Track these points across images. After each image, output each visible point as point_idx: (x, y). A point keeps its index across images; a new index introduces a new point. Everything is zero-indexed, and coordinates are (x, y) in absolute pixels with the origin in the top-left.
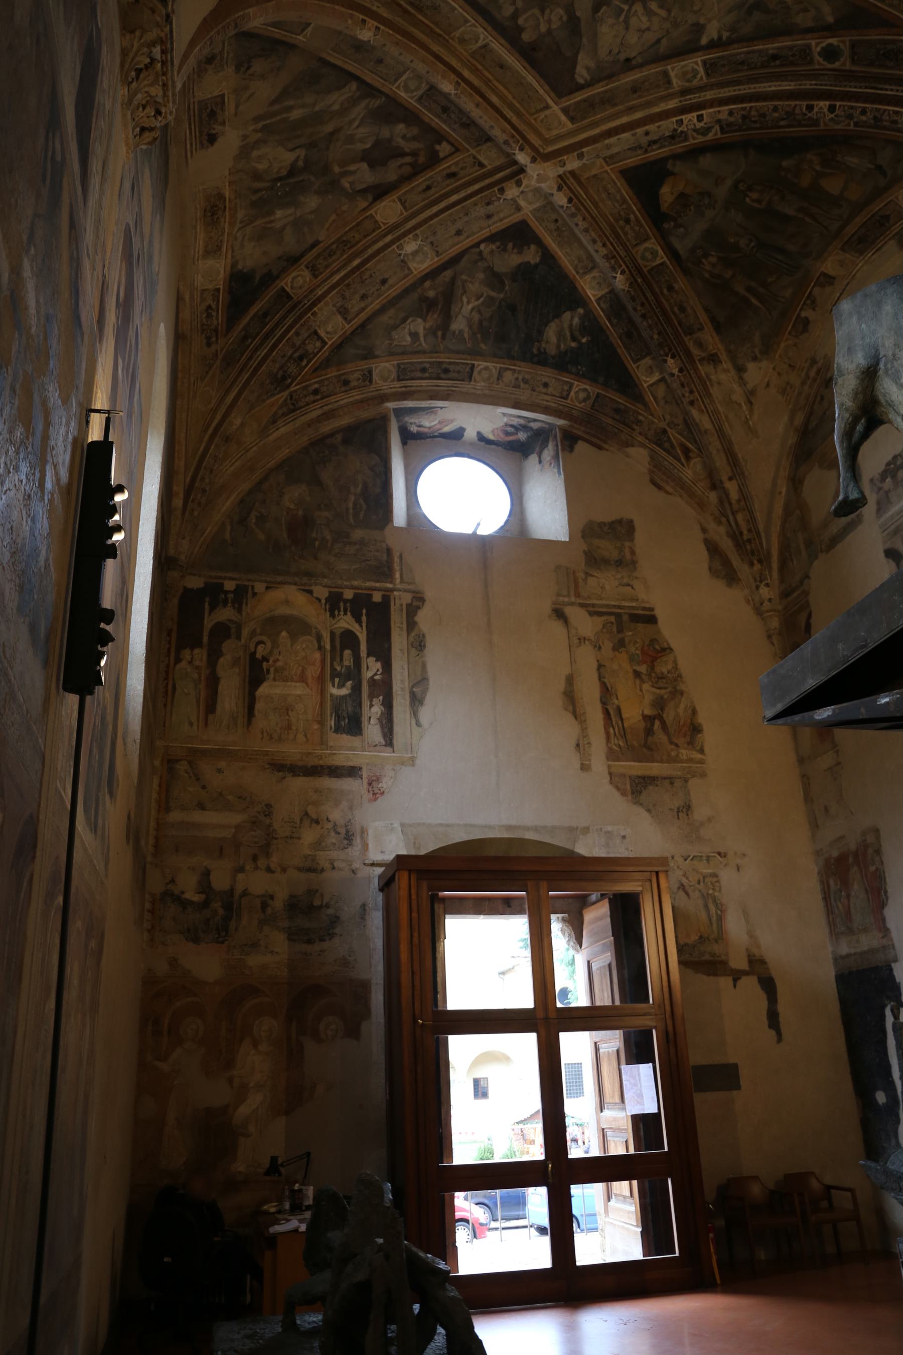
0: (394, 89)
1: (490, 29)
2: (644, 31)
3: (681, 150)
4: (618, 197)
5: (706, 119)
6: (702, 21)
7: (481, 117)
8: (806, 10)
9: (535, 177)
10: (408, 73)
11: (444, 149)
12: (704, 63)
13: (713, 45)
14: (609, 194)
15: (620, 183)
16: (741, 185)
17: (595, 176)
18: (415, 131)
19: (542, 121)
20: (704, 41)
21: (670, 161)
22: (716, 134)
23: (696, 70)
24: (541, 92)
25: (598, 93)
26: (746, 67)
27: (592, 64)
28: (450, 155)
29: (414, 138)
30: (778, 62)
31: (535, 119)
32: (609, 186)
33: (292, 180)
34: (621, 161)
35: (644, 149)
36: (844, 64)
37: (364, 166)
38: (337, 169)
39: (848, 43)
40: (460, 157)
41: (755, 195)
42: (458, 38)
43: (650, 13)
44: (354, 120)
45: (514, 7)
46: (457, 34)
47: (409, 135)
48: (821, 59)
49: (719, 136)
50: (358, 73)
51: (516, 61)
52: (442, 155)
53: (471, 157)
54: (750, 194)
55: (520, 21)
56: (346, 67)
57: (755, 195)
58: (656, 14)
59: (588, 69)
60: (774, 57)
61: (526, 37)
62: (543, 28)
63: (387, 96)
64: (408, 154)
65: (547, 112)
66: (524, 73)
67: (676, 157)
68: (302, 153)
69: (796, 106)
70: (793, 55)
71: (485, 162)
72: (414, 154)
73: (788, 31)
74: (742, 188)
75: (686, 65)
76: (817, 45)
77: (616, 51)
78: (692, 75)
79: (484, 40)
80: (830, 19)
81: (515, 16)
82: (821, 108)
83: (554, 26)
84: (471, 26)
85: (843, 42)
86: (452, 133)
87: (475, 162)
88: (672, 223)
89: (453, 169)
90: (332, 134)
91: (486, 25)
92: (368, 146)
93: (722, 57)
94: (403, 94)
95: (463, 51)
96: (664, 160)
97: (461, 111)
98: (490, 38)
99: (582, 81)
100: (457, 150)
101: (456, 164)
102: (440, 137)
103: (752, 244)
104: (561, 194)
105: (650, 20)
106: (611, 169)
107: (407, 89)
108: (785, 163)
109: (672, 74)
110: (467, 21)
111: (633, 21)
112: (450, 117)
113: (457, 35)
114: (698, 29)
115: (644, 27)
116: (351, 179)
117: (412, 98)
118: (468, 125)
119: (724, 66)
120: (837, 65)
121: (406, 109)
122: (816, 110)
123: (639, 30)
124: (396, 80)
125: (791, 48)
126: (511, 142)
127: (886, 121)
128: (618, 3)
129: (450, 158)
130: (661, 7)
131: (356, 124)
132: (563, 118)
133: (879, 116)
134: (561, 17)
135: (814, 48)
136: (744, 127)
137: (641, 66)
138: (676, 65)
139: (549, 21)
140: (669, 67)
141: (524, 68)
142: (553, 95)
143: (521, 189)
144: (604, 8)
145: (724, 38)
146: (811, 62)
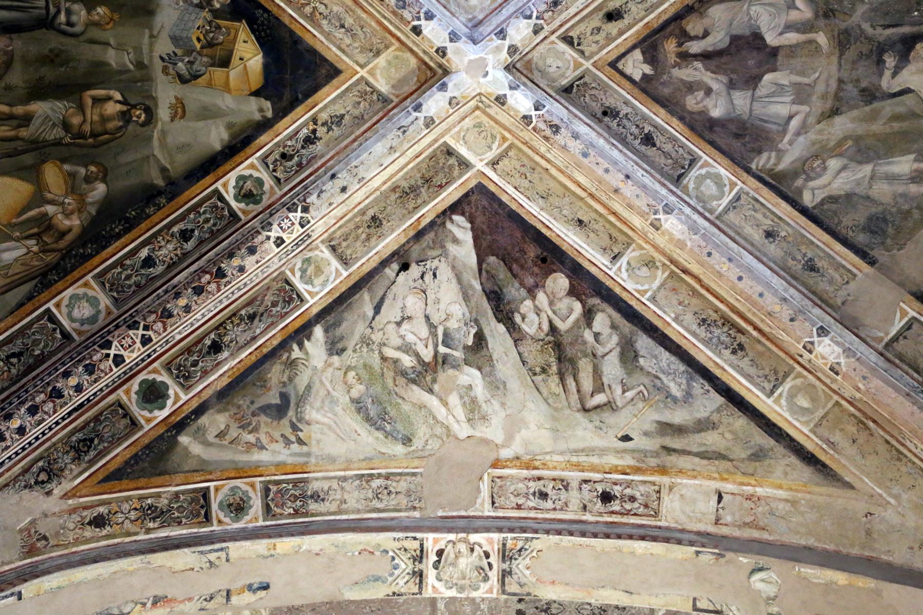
0: (739, 182)
1: (617, 290)
2: (403, 319)
3: (263, 139)
4: (324, 22)
5: (271, 244)
6: (336, 358)
7: (607, 171)
8: (221, 435)
9: (489, 69)
10: (721, 208)
11: (636, 66)
12: (302, 300)
13: (302, 333)
14: (342, 26)
15: (331, 52)
16: (143, 117)
17: (378, 53)
18: (692, 102)
19: (493, 137)
20: (318, 331)
21: (269, 114)
22: (225, 185)
23: (306, 283)
24: (510, 190)
25: (425, 203)
26: (243, 312)
27: (452, 248)
28: (624, 55)
29: (691, 87)
30: (208, 342)
31: (504, 139)
32: (348, 41)
33: (906, 30)
34: (347, 89)
35: (319, 123)
36: (127, 392)
37: (771, 39)
38: (822, 39)
39: (143, 422)
40: (605, 51)
41: (112, 108)
42: (657, 268)
43: (407, 348)
44: (798, 134)
45: (594, 329)
46: (661, 276)
47: (700, 94)
48: (159, 379)
49: (219, 185)
50: (803, 220)
51: (563, 236)
52: (637, 54)
53: (587, 54)
54: (119, 107)
55: (578, 307)
56: (826, 237)
57: (112, 108)
58: (399, 349)
59: (456, 241)
60: (216, 348)
61: (560, 282)
62: (541, 297)
63: (748, 171)
64: (696, 56)
65: (490, 155)
66: (544, 217)
67: (265, 125)
68: (887, 83)
69: (165, 330)
70: (195, 364)
71: (563, 47)
72: (685, 57)
73: (224, 395)
74: (138, 113)
75: (324, 285)
76: (177, 398)
77: (428, 277)
78: (308, 273)
79: (620, 269)
80: (184, 439)
81: (588, 315)
82: (133, 351)
83: (528, 303)
84: (646, 292)
85: (149, 421)
86: (629, 97)
87: (579, 44)
88: (218, 6)
89: (613, 28)
90: (835, 112)
91: (624, 296)
92: (768, 77)
93: (283, 316)
94: (723, 172)
95: (644, 245)
96: (281, 112)
97: (623, 141)
98: (611, 273)
99: (455, 217)
100: (613, 65)
101: (610, 39)
102: (645, 87)
103: (62, 18)
104: (438, 44)
105: (402, 337)
106: (357, 73)
107: (717, 180)
108: (100, 189)
109: (335, 263)
110: (653, 299)
111: (424, 332)
112: (637, 126)
113: (659, 272)
114: (335, 348)
115: (405, 326)
116: (794, 15)
117: (706, 164)
118: (605, 113)
119: (274, 304)
120: (135, 385)
121: (712, 143)
122: (138, 345)
123: (409, 318)
124: (738, 198)
125: (205, 373)
126: (548, 132)
127: (44, 402)
128: (455, 353)
129: (623, 50)
130: (396, 361)
131: (794, 123)
132: (463, 151)
133: (58, 401)
134: (523, 319)
135: (178, 390)
136: (192, 216)
137: (384, 263)
138: (338, 281)
139: (538, 311)
140: (345, 274)
141: (548, 227)
142: (492, 188)
143: (507, 43)
144: (470, 342)
145: (295, 347)
146: (168, 367)
